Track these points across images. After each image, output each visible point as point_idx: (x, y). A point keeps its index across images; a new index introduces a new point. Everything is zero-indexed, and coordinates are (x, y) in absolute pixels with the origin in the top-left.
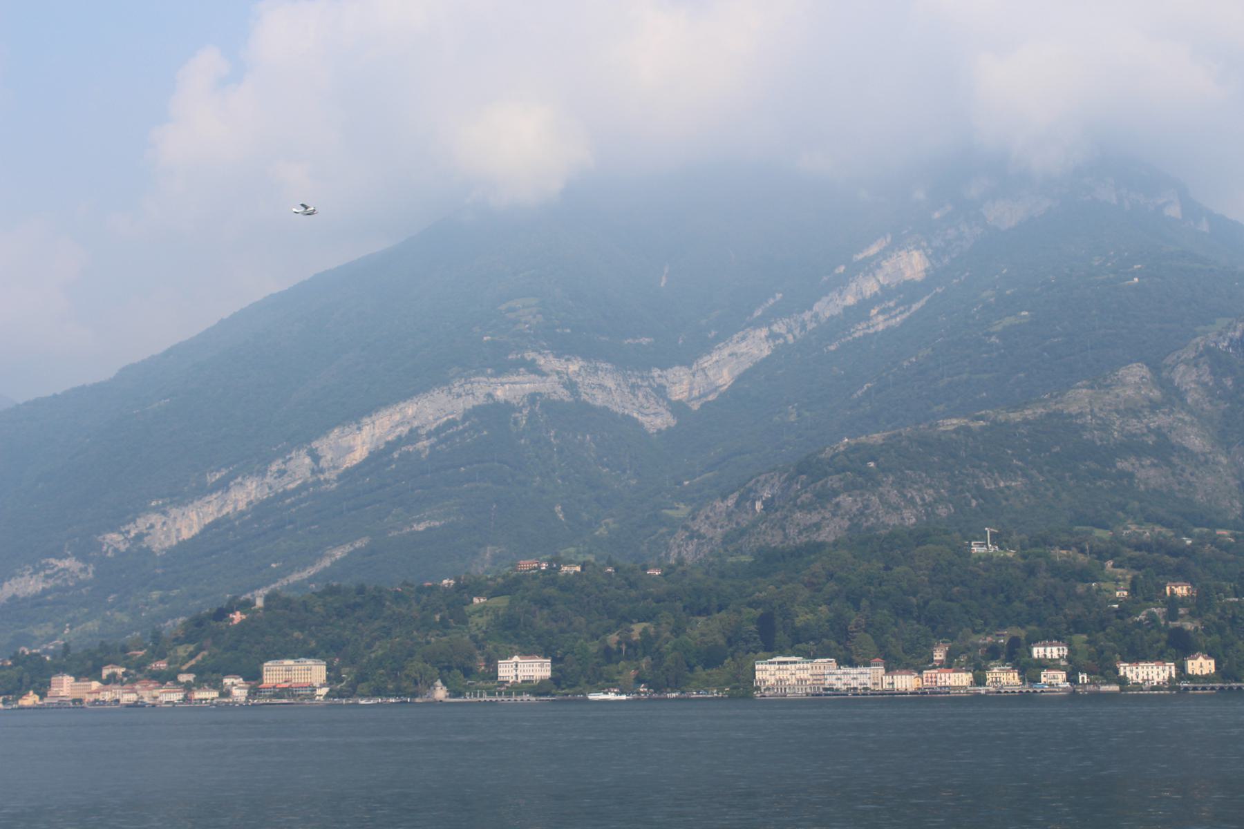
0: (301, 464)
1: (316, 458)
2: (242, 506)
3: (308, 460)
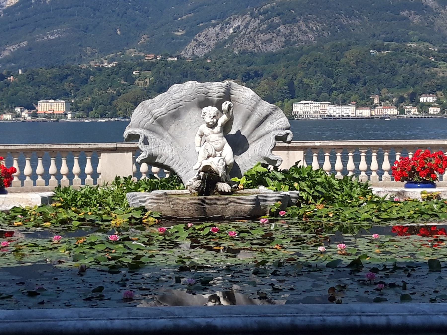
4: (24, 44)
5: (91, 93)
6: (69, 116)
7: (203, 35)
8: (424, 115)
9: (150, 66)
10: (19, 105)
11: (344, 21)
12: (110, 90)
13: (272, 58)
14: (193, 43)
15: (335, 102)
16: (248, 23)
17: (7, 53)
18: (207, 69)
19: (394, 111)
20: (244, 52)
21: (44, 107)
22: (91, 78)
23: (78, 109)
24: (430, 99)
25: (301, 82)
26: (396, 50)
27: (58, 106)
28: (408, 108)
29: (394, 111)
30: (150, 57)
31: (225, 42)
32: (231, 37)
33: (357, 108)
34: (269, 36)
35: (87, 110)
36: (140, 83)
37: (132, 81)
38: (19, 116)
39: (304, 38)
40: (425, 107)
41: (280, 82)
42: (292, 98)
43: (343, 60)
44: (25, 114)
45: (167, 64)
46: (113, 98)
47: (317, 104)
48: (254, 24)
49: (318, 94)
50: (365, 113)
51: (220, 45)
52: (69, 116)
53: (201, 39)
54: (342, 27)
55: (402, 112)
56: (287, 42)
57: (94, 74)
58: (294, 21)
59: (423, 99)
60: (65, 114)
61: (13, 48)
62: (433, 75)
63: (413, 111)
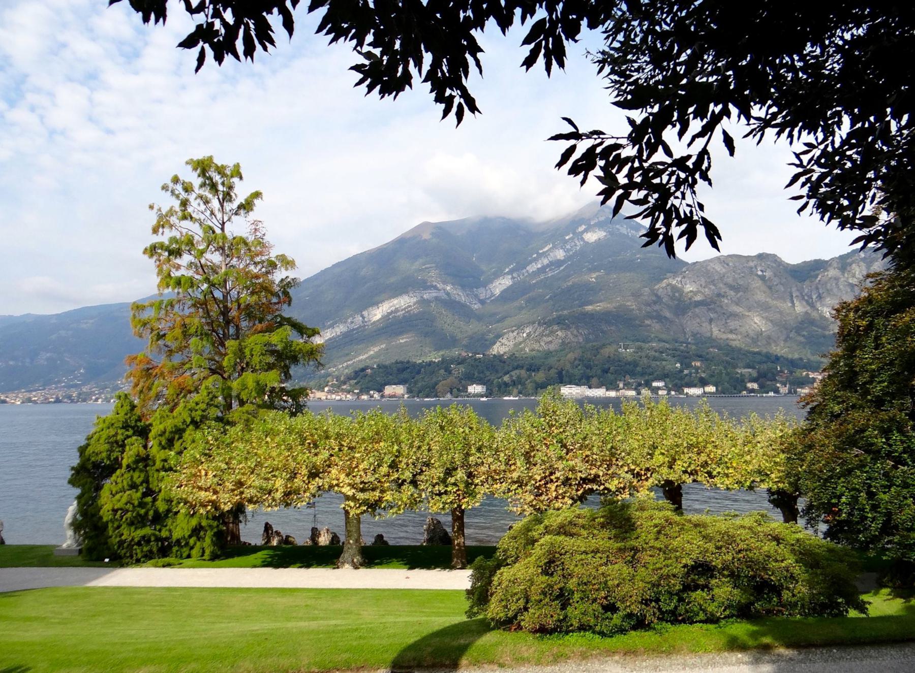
2: (338, 333)
4: (383, 346)
6: (406, 396)
10: (374, 389)
14: (498, 344)
17: (372, 353)
21: (389, 390)
24: (660, 384)
27: (400, 390)
32: (525, 340)
33: (607, 390)
34: (550, 339)
38: (372, 397)
41: (553, 371)
44: (377, 396)
45: (476, 360)
47: (579, 388)
50: (612, 394)
53: (503, 341)
54: (603, 332)
55: (639, 393)
59: (655, 384)
61: (376, 349)
63: (645, 392)
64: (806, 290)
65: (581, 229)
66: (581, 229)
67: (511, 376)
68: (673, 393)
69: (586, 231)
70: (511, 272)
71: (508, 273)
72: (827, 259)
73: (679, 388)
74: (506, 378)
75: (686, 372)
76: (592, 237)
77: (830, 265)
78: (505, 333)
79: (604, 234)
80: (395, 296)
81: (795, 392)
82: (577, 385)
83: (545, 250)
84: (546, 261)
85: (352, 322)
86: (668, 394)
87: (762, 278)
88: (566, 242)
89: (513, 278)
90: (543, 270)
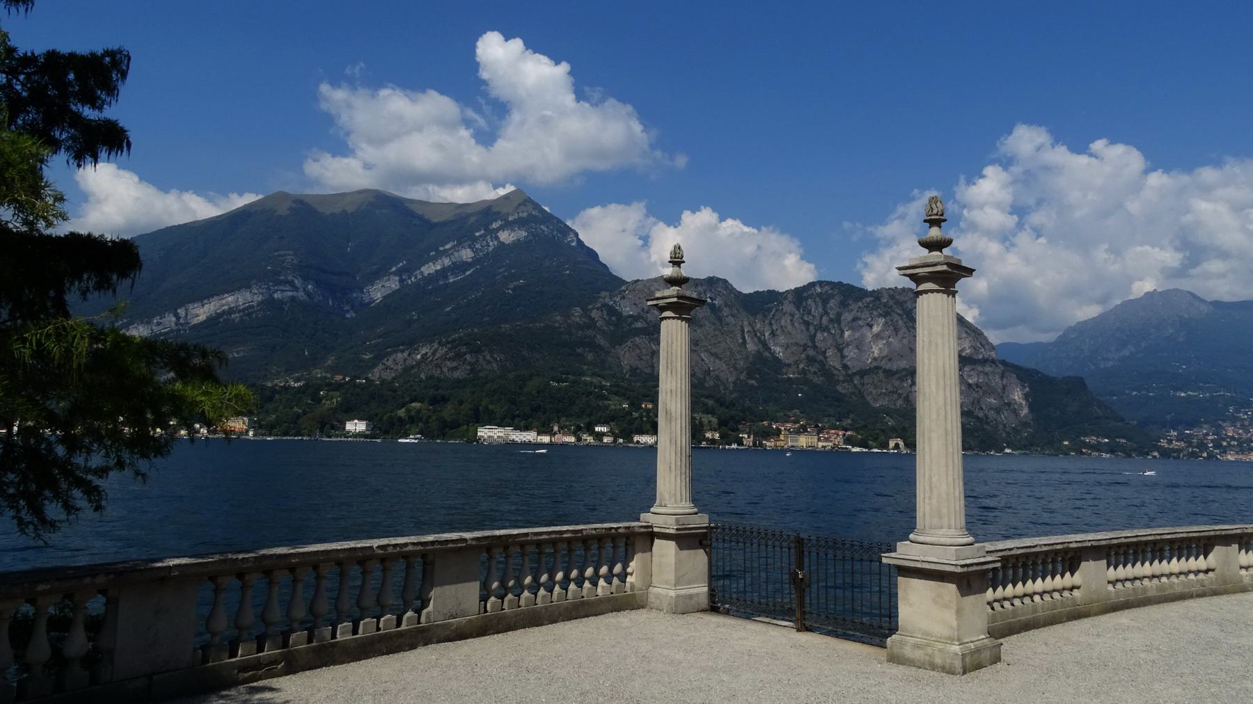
0: (170, 319)
1: (178, 318)
3: (174, 319)
5: (276, 410)
6: (251, 433)
7: (391, 360)
8: (598, 443)
9: (339, 387)
10: (198, 422)
11: (525, 353)
12: (296, 409)
13: (459, 384)
14: (381, 366)
15: (517, 428)
16: (436, 350)
18: (395, 391)
19: (571, 439)
20: (431, 377)
22: (277, 396)
23: (261, 427)
24: (604, 429)
25: (487, 408)
26: (574, 382)
28: (585, 437)
29: (571, 439)
30: (338, 378)
31: (412, 367)
32: (419, 363)
34: (455, 364)
35: (270, 429)
36: (327, 404)
37: (318, 400)
39: (489, 367)
40: (600, 436)
42: (477, 422)
43: (526, 390)
45: (355, 386)
46: (298, 416)
47: (501, 429)
48: (442, 351)
49: (503, 419)
50: (546, 439)
51: (407, 370)
52: (251, 433)
53: (390, 363)
55: (579, 439)
56: (472, 370)
57: (280, 393)
58: (477, 351)
59: (597, 429)
60: (247, 432)
62: (607, 407)
63: (590, 439)
64: (758, 326)
65: (495, 225)
66: (495, 225)
67: (408, 411)
68: (621, 441)
69: (502, 228)
70: (399, 273)
71: (395, 274)
72: (781, 291)
73: (628, 436)
74: (401, 413)
75: (635, 415)
76: (506, 237)
77: (785, 298)
78: (390, 354)
79: (524, 234)
80: (230, 291)
81: (761, 445)
82: (500, 425)
83: (448, 247)
84: (447, 262)
85: (159, 324)
86: (615, 441)
87: (712, 307)
88: (476, 239)
89: (401, 281)
90: (443, 273)
